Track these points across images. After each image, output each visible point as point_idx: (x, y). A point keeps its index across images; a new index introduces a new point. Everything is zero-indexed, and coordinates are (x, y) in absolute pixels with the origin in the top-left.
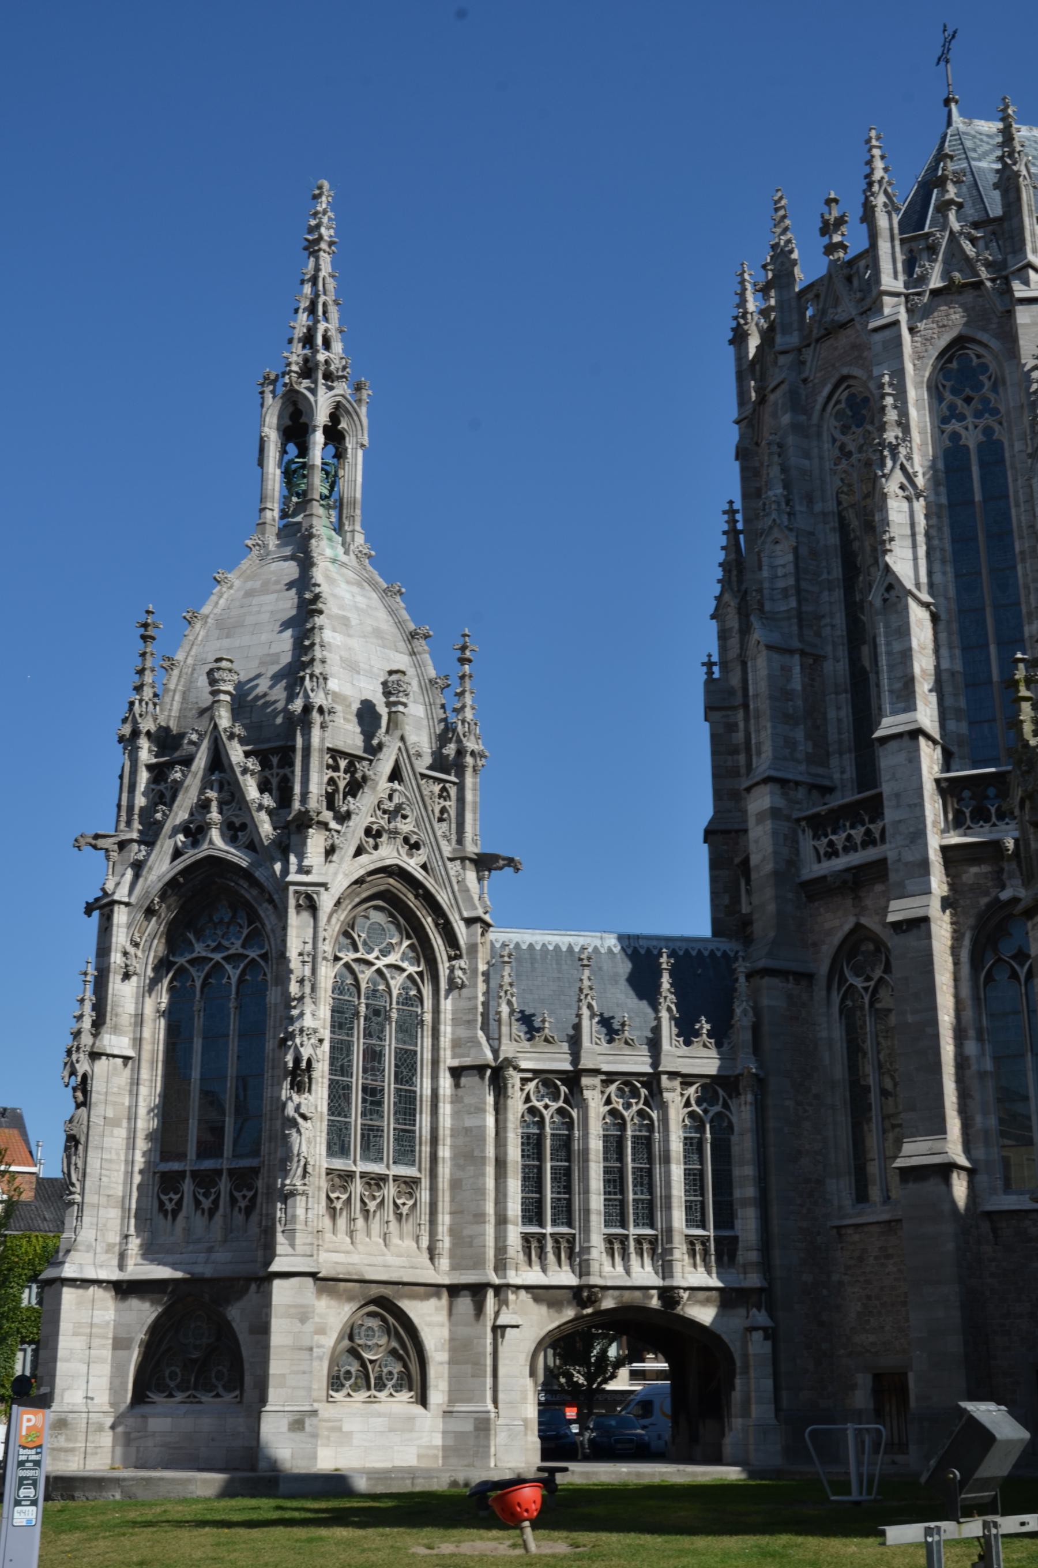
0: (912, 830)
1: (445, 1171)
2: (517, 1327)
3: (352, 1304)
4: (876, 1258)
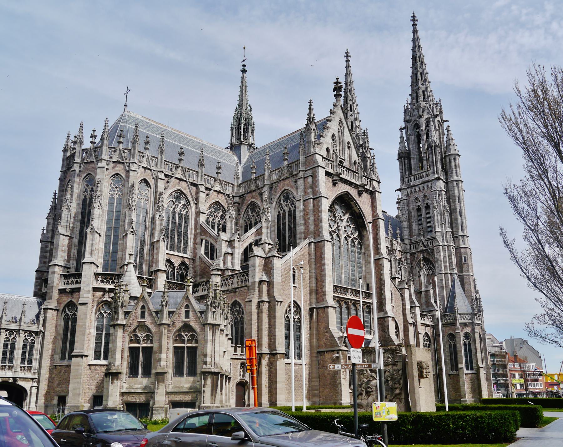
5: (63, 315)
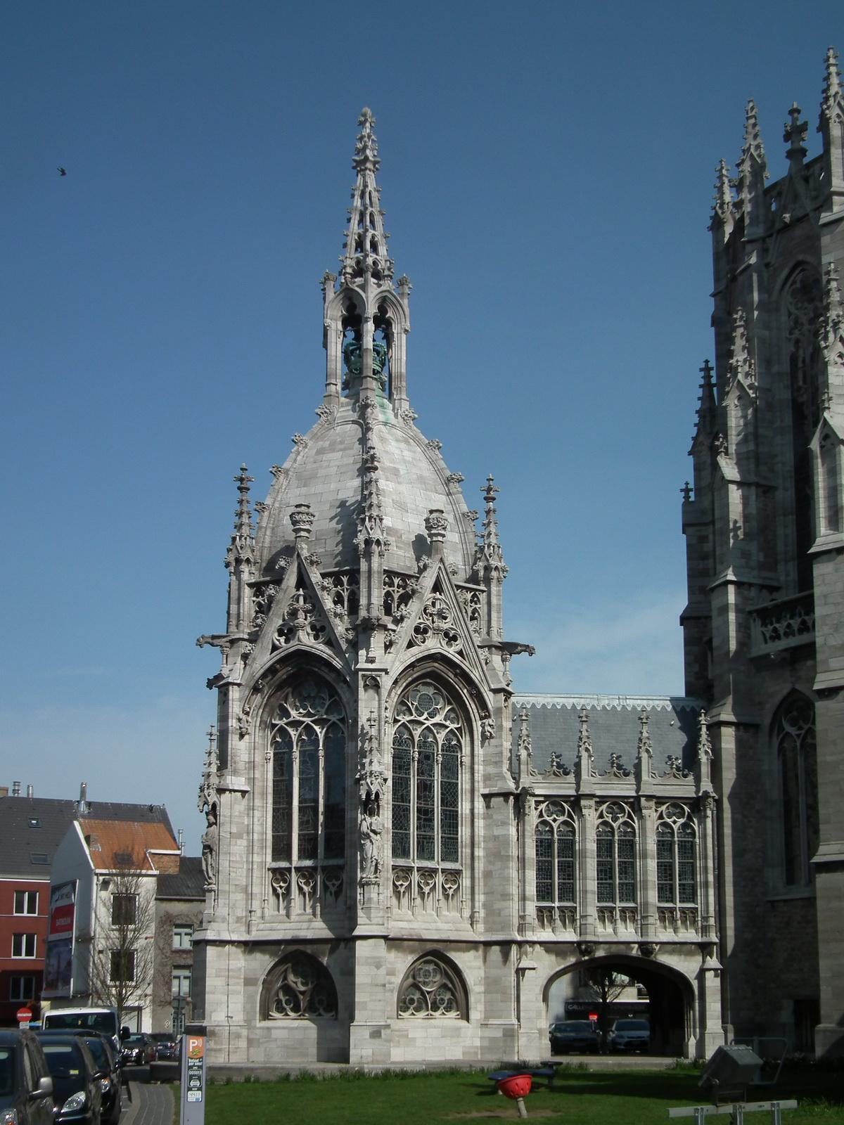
1: (480, 866)
2: (534, 969)
3: (413, 956)
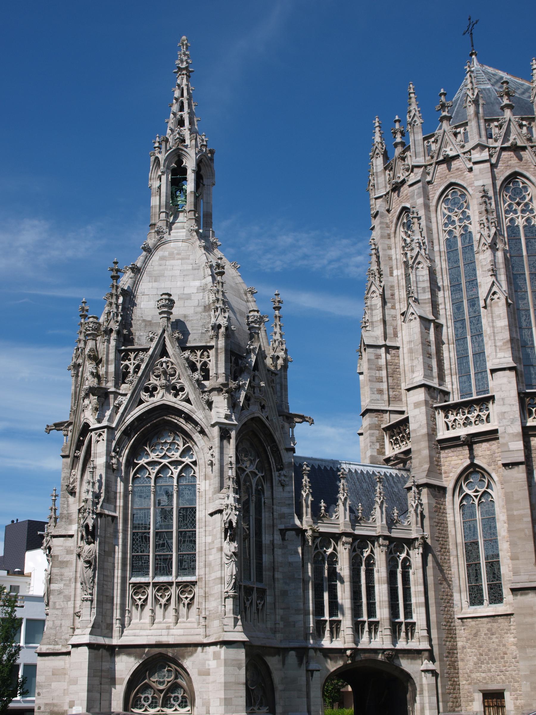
0: (511, 417)
2: (319, 670)
4: (485, 634)
5: (457, 500)
